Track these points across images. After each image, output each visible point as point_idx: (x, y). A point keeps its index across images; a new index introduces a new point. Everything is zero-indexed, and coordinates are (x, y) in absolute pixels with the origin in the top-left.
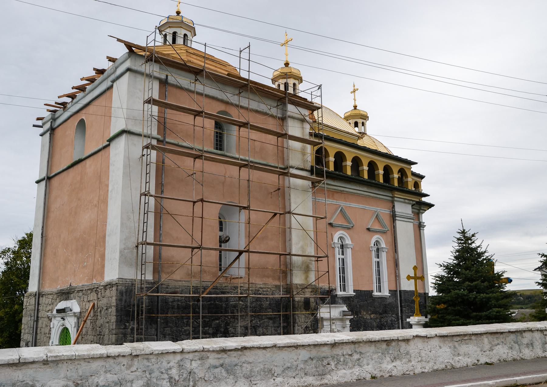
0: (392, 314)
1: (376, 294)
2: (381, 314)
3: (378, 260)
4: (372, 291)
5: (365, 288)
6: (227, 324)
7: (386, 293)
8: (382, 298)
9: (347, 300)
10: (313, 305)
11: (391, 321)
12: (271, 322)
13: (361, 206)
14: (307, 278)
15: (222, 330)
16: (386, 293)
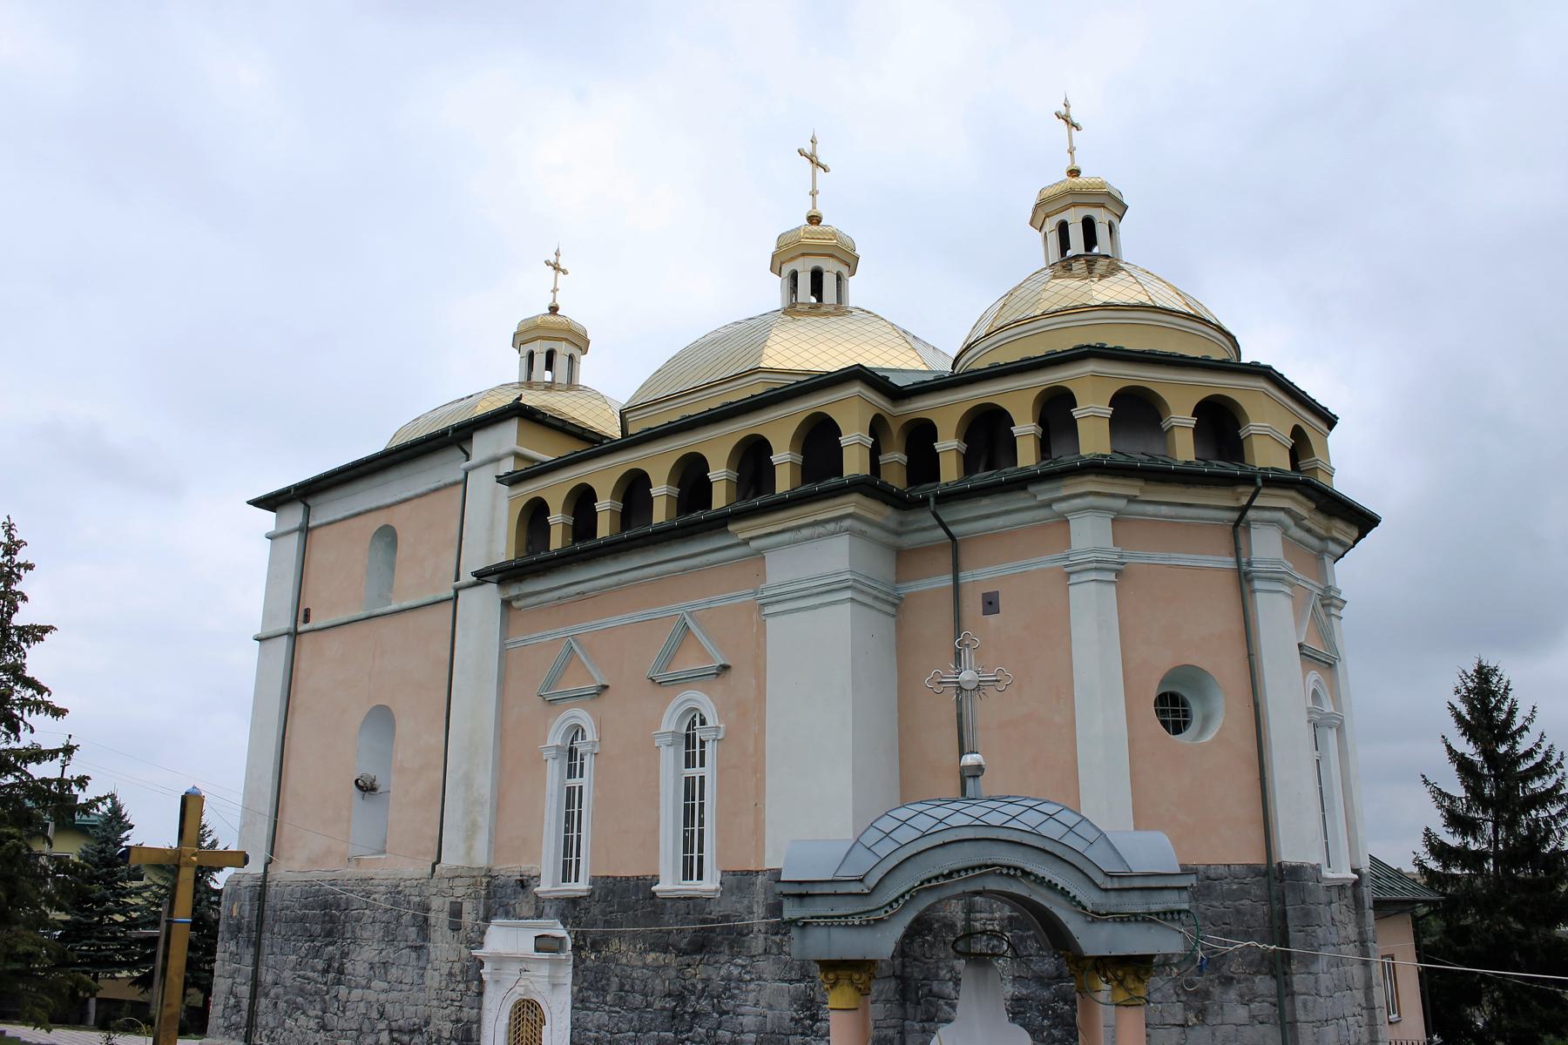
0: (733, 956)
1: (669, 883)
2: (681, 953)
3: (695, 772)
4: (655, 880)
5: (629, 868)
6: (344, 955)
7: (709, 884)
8: (692, 903)
9: (570, 908)
10: (468, 918)
11: (728, 979)
12: (414, 955)
13: (637, 616)
14: (470, 849)
15: (336, 965)
16: (709, 884)
